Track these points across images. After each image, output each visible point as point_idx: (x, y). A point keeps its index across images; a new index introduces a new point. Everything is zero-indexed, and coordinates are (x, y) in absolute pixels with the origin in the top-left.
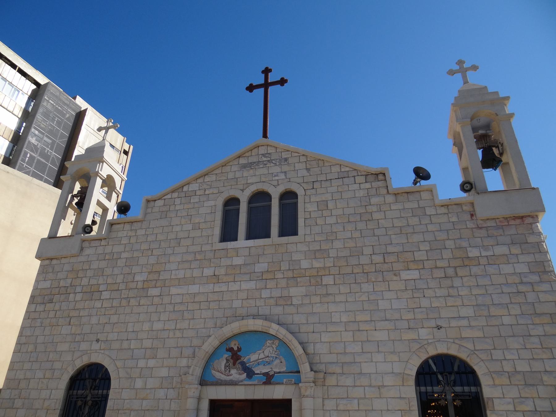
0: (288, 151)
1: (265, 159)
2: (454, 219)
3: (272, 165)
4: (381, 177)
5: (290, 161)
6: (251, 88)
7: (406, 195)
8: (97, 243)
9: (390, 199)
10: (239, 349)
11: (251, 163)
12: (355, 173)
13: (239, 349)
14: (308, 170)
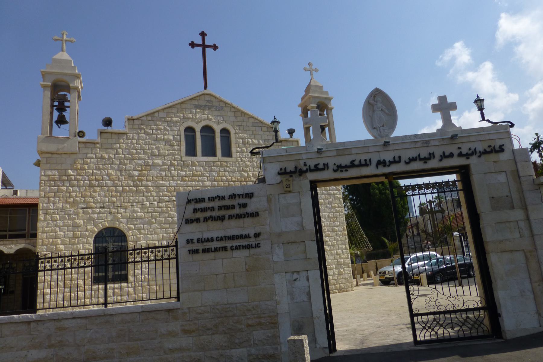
1: (209, 104)
3: (214, 109)
5: (226, 109)
6: (193, 45)
8: (93, 146)
12: (261, 125)
14: (236, 117)
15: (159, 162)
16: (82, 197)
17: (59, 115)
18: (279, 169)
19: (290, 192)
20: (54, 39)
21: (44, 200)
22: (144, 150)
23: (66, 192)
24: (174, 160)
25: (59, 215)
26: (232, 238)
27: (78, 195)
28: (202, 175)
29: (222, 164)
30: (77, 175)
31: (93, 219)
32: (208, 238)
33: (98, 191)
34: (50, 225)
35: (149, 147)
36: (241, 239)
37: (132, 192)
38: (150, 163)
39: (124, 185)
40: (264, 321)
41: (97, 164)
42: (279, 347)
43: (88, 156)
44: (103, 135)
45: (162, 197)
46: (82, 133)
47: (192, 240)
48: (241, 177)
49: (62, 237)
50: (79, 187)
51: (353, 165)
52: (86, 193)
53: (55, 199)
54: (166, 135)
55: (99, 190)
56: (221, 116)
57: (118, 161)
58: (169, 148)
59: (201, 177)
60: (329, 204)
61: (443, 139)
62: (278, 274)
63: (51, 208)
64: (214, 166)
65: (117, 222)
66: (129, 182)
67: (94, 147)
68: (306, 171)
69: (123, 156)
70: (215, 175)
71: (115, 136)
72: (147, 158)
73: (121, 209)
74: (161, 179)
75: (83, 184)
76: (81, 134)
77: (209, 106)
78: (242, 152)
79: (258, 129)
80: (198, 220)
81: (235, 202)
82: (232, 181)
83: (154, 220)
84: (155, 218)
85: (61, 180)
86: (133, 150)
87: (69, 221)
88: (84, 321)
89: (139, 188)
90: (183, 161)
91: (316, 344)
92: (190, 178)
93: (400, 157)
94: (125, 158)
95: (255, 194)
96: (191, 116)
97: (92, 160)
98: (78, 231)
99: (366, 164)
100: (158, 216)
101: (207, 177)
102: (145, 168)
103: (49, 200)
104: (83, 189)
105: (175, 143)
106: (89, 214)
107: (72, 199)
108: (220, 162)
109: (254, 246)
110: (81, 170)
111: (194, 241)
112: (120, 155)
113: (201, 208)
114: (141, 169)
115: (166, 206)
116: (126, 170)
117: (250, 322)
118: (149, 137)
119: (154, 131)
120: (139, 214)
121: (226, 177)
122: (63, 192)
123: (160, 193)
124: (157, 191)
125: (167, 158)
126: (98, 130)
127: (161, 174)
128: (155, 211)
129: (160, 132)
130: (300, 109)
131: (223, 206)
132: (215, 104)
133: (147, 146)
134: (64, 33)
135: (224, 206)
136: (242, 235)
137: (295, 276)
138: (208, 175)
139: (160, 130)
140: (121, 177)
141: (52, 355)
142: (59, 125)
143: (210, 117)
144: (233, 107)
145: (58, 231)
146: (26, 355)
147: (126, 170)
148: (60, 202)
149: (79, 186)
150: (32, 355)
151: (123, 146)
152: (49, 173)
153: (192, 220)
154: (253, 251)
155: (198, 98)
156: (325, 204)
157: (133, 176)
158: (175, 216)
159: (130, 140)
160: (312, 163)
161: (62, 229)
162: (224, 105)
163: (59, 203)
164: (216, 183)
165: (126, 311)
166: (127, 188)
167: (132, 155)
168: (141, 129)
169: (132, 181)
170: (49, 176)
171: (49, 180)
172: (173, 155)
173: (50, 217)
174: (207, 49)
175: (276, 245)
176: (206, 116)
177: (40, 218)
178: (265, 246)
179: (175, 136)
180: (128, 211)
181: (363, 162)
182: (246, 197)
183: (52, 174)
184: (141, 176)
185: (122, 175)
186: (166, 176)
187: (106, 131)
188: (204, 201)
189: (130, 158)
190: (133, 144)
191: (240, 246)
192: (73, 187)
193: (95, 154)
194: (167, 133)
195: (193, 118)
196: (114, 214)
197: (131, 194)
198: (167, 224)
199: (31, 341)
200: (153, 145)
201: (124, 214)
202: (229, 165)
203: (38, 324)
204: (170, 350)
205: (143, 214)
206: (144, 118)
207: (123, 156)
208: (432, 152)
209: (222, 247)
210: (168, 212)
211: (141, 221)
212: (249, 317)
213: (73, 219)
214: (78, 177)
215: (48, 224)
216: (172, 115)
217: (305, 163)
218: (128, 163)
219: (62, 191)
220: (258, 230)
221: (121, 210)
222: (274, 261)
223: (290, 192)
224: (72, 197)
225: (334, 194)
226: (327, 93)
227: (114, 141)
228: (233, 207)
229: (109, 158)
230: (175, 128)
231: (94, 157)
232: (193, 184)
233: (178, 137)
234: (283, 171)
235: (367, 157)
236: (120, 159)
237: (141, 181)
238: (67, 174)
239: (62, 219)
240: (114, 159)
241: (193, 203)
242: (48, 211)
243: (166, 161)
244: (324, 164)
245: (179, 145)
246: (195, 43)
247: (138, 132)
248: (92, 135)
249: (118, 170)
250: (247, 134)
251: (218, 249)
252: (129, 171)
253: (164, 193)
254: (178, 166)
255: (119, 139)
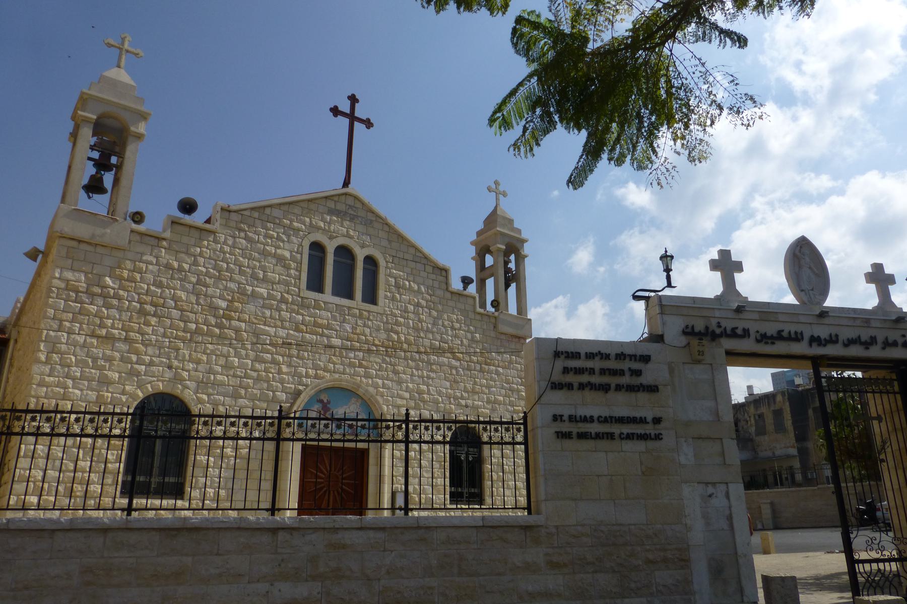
0: (373, 213)
1: (352, 212)
2: (485, 327)
3: (358, 222)
4: (444, 273)
7: (458, 295)
8: (154, 242)
9: (448, 295)
10: (329, 402)
11: (338, 210)
12: (424, 261)
13: (329, 402)
14: (390, 242)
15: (263, 291)
16: (122, 330)
17: (92, 177)
18: (683, 326)
19: (699, 361)
20: (106, 42)
21: (52, 324)
22: (240, 266)
23: (95, 316)
24: (288, 293)
25: (76, 356)
26: (621, 420)
27: (116, 326)
28: (328, 327)
29: (361, 314)
30: (119, 289)
31: (138, 374)
32: (585, 417)
33: (153, 323)
34: (56, 374)
35: (250, 262)
36: (634, 423)
37: (212, 337)
38: (248, 291)
39: (200, 320)
40: (670, 556)
41: (158, 276)
42: (692, 599)
43: (144, 258)
44: (176, 227)
45: (261, 352)
46: (138, 216)
47: (561, 416)
48: (388, 340)
49: (75, 398)
50: (121, 311)
51: (779, 337)
52: (132, 324)
53: (73, 325)
54: (279, 247)
55: (156, 322)
56: (366, 234)
57: (194, 277)
58: (282, 272)
59: (326, 329)
60: (510, 405)
61: (885, 320)
62: (688, 484)
63: (63, 340)
64: (348, 315)
65: (180, 386)
66: (209, 317)
67: (156, 245)
68: (721, 335)
69: (204, 270)
70: (348, 329)
71: (196, 234)
72: (245, 282)
73: (190, 363)
74: (262, 321)
75: (128, 308)
76: (138, 217)
77: (351, 214)
78: (393, 299)
79: (419, 266)
80: (570, 386)
81: (626, 365)
82: (374, 345)
83: (243, 392)
84: (246, 389)
85: (89, 292)
86: (221, 263)
87: (93, 371)
88: (380, 535)
89: (226, 330)
90: (302, 298)
91: (742, 596)
92: (310, 329)
93: (837, 336)
94: (207, 274)
95: (653, 358)
96: (322, 224)
97: (150, 267)
98: (108, 391)
99: (797, 338)
100: (252, 385)
101: (336, 331)
102: (238, 298)
103: (60, 325)
104: (126, 315)
105: (293, 265)
106: (131, 363)
107: (104, 332)
108: (359, 310)
109: (653, 436)
110: (127, 280)
111: (564, 418)
112: (200, 268)
113: (575, 368)
114: (232, 299)
115: (266, 371)
116: (206, 295)
117: (651, 557)
118: (251, 246)
119: (261, 238)
120: (219, 377)
121: (366, 336)
122: (89, 316)
123: (258, 345)
124: (255, 340)
125: (277, 288)
126: (169, 216)
127: (263, 313)
128: (246, 376)
129: (270, 241)
130: (474, 248)
131: (608, 369)
132: (362, 213)
133: (247, 260)
134: (125, 37)
135: (609, 370)
136: (636, 418)
137: (710, 490)
138: (338, 329)
139: (271, 237)
140: (196, 306)
141: (318, 593)
142: (91, 194)
143: (351, 233)
144: (387, 224)
145: (71, 386)
146: (267, 592)
147: (206, 295)
148: (81, 332)
149: (120, 309)
150: (280, 591)
151: (206, 253)
152: (69, 275)
153: (562, 384)
154: (651, 444)
155: (336, 199)
156: (505, 404)
157: (217, 308)
158: (279, 390)
159: (219, 245)
160: (729, 325)
161: (79, 383)
162: (374, 219)
163: (79, 334)
164: (349, 343)
165: (457, 523)
166: (205, 328)
167: (219, 272)
168: (240, 230)
169: (214, 316)
170: (68, 281)
171: (66, 289)
172: (287, 284)
173: (58, 357)
174: (356, 124)
175: (683, 440)
176: (345, 230)
177: (40, 357)
178: (669, 439)
179: (294, 254)
180: (200, 368)
181: (793, 336)
182: (640, 360)
183: (73, 278)
184: (230, 311)
185: (198, 304)
186: (271, 317)
187: (182, 221)
188: (580, 358)
189: (215, 275)
190: (224, 253)
191: (633, 434)
192: (110, 310)
193: (157, 257)
194: (281, 244)
195: (324, 230)
196: (176, 369)
197: (210, 339)
198: (264, 401)
199: (280, 565)
200: (256, 261)
201: (193, 373)
202: (371, 317)
203: (292, 535)
204: (530, 594)
205: (225, 377)
206: (247, 213)
207: (204, 270)
208: (873, 335)
209: (607, 433)
210: (268, 382)
211: (221, 389)
212: (648, 547)
213: (101, 368)
214: (121, 292)
215: (52, 370)
216: (292, 217)
217: (719, 323)
218: (211, 284)
219: (88, 314)
220: (658, 415)
221: (189, 366)
222: (682, 463)
223: (699, 362)
224: (105, 328)
225: (518, 391)
226: (519, 231)
227: (193, 241)
228: (621, 373)
229: (180, 269)
230: (294, 239)
231: (155, 262)
232: (313, 339)
233: (299, 256)
234: (689, 330)
235: (799, 328)
236: (198, 275)
237: (230, 318)
238: (102, 284)
239: (80, 365)
240: (189, 272)
241: (563, 357)
242: (57, 345)
243: (275, 293)
244: (744, 330)
245: (299, 269)
246: (340, 109)
247: (234, 234)
248: (154, 223)
249: (192, 293)
250: (403, 272)
251: (601, 435)
252: (211, 298)
253: (264, 346)
254: (292, 303)
255: (201, 239)
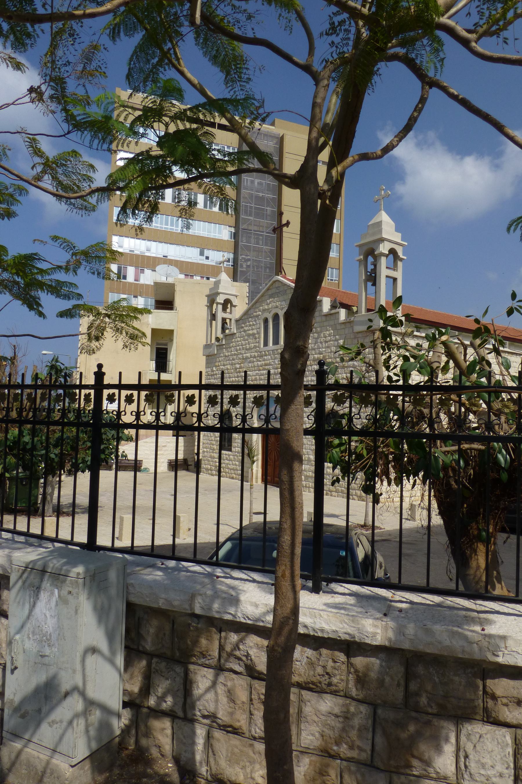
9: (324, 318)
15: (248, 355)
44: (228, 337)
105: (257, 336)
